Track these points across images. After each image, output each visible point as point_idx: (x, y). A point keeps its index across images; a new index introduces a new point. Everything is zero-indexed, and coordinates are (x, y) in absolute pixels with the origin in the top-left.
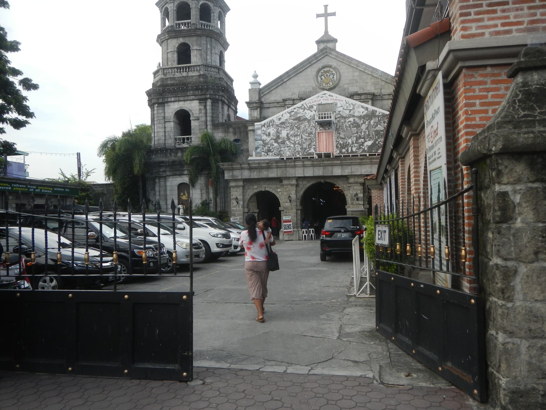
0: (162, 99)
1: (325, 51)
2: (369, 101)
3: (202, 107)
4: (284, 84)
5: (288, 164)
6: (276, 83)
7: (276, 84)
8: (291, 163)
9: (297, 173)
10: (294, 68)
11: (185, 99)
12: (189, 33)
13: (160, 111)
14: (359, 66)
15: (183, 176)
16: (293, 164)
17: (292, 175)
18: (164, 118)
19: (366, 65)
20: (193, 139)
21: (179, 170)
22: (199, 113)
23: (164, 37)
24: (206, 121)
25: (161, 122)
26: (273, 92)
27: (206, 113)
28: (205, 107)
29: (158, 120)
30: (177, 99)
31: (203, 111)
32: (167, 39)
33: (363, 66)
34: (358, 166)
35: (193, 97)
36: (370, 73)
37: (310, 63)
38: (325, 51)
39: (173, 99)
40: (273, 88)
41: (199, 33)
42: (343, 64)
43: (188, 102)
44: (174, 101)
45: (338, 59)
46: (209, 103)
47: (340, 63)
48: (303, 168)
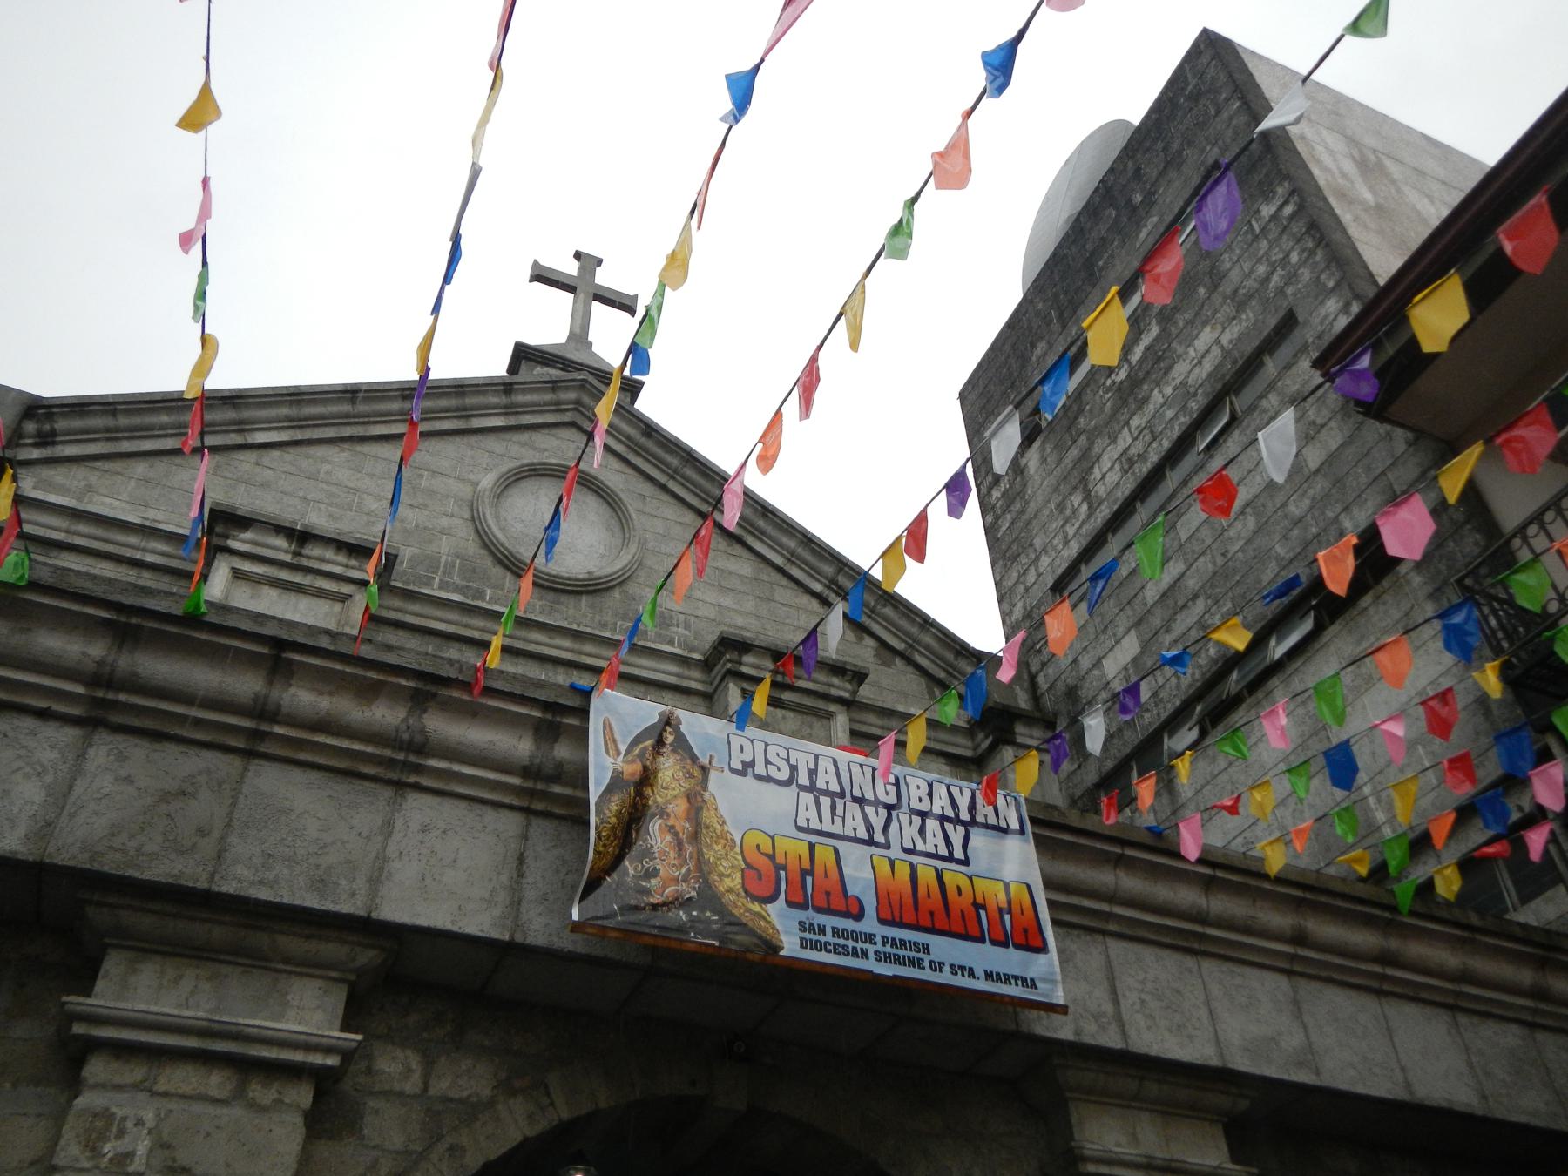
1: (572, 395)
2: (829, 716)
4: (246, 460)
5: (302, 698)
8: (368, 692)
9: (405, 872)
10: (351, 393)
14: (760, 534)
16: (386, 715)
17: (320, 884)
19: (808, 540)
26: (140, 468)
33: (785, 540)
34: (1172, 960)
36: (818, 587)
37: (464, 413)
38: (572, 395)
40: (148, 445)
42: (666, 497)
45: (638, 462)
47: (647, 488)
48: (509, 823)
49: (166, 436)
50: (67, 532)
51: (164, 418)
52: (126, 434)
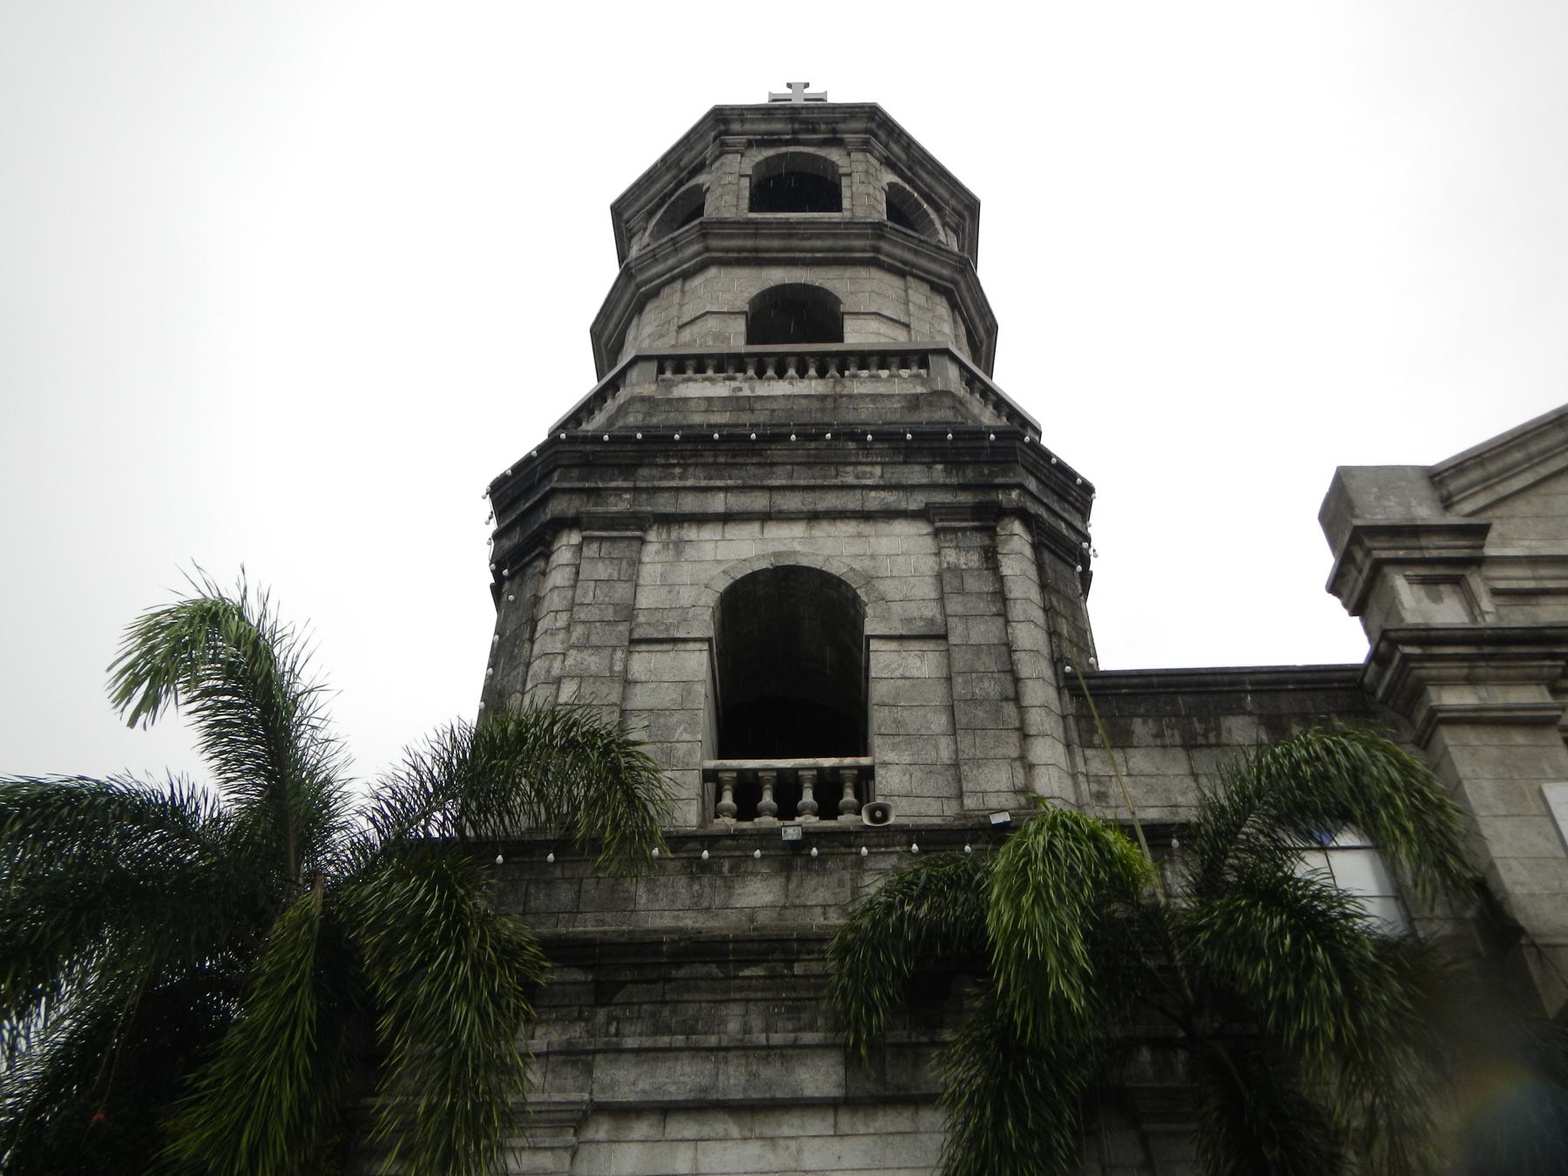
0: (633, 502)
3: (974, 560)
6: (1534, 448)
7: (1531, 462)
11: (821, 506)
12: (841, 243)
13: (603, 571)
15: (789, 1126)
18: (628, 612)
20: (889, 782)
21: (745, 1048)
22: (941, 599)
23: (671, 262)
24: (1009, 648)
25: (594, 640)
27: (1001, 596)
28: (991, 558)
29: (568, 629)
30: (759, 502)
31: (979, 584)
32: (687, 276)
35: (891, 499)
39: (718, 503)
41: (898, 252)
43: (847, 528)
44: (727, 518)
46: (1017, 544)
49: (1524, 470)
50: (1534, 578)
51: (1518, 456)
52: (1496, 480)
